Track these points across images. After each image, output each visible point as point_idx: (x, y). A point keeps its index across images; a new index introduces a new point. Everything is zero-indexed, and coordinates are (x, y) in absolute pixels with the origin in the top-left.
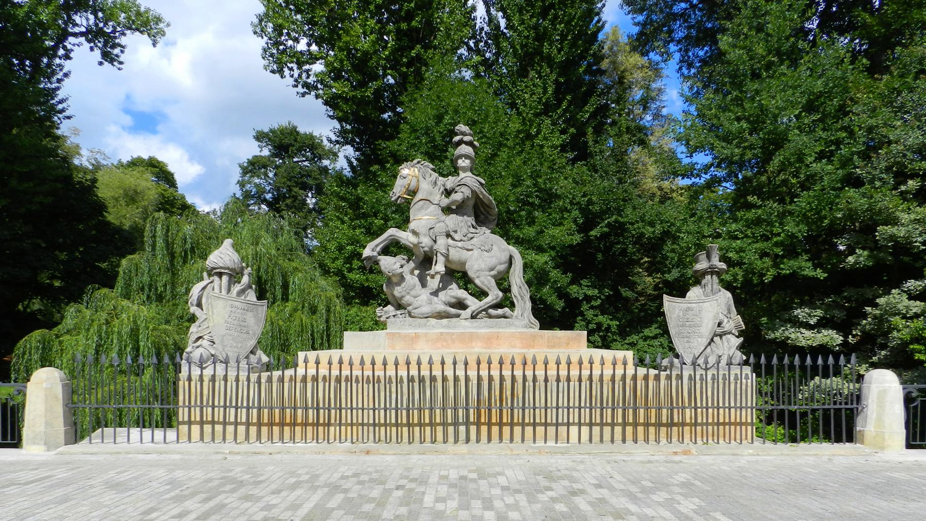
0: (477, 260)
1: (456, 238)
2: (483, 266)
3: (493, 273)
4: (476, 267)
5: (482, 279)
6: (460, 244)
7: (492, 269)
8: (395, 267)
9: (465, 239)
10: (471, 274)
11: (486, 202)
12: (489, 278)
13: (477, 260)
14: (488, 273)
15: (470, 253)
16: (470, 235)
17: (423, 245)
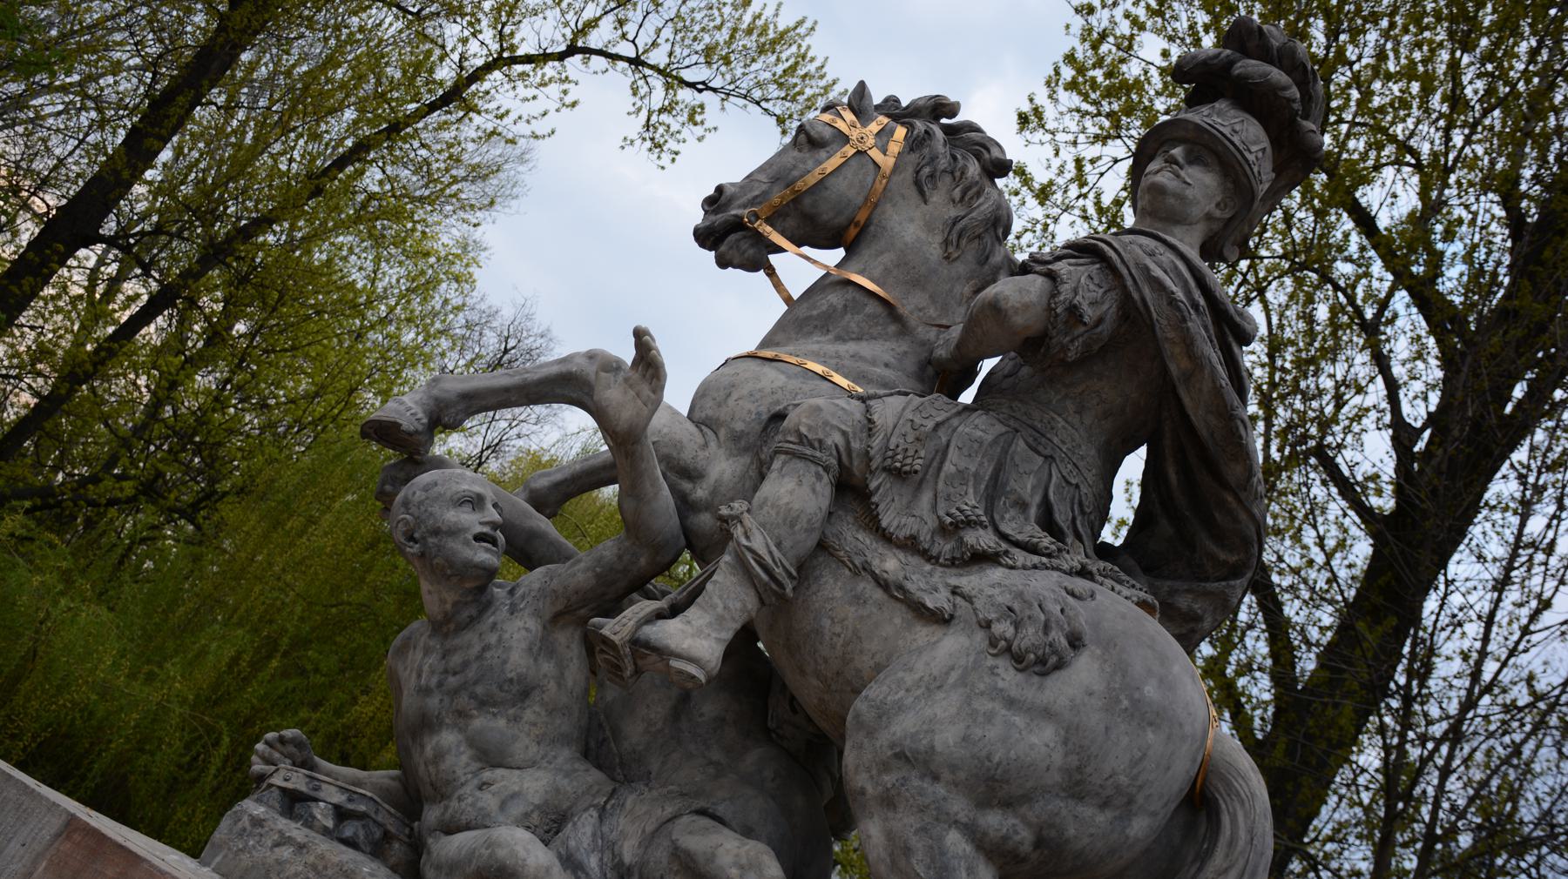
0: (934, 685)
1: (887, 520)
2: (947, 738)
3: (994, 821)
4: (903, 726)
5: (906, 822)
6: (891, 563)
7: (994, 786)
8: (453, 516)
9: (946, 547)
10: (858, 764)
11: (1199, 417)
12: (955, 841)
13: (934, 685)
14: (959, 806)
15: (923, 633)
16: (983, 539)
17: (700, 492)
